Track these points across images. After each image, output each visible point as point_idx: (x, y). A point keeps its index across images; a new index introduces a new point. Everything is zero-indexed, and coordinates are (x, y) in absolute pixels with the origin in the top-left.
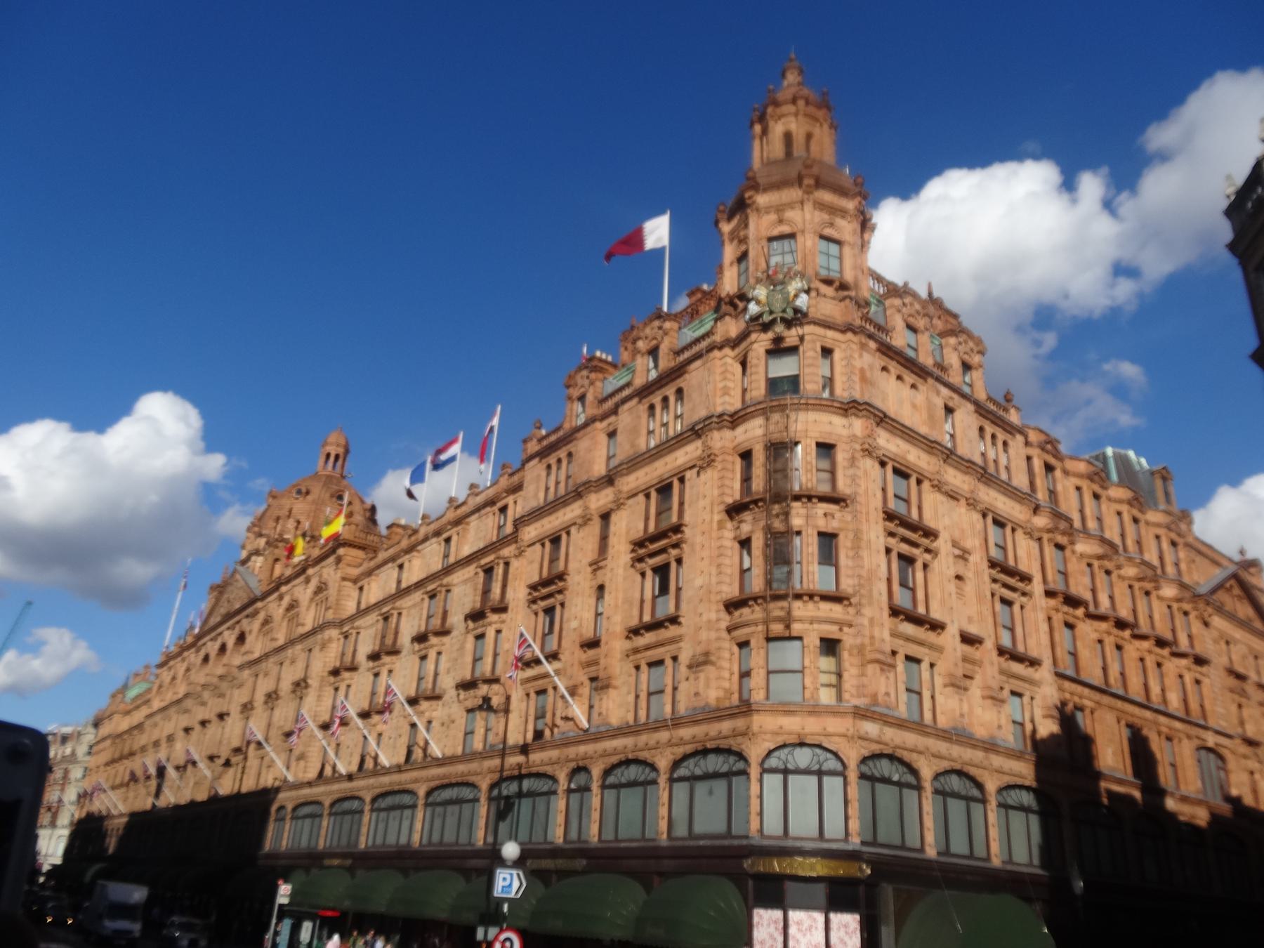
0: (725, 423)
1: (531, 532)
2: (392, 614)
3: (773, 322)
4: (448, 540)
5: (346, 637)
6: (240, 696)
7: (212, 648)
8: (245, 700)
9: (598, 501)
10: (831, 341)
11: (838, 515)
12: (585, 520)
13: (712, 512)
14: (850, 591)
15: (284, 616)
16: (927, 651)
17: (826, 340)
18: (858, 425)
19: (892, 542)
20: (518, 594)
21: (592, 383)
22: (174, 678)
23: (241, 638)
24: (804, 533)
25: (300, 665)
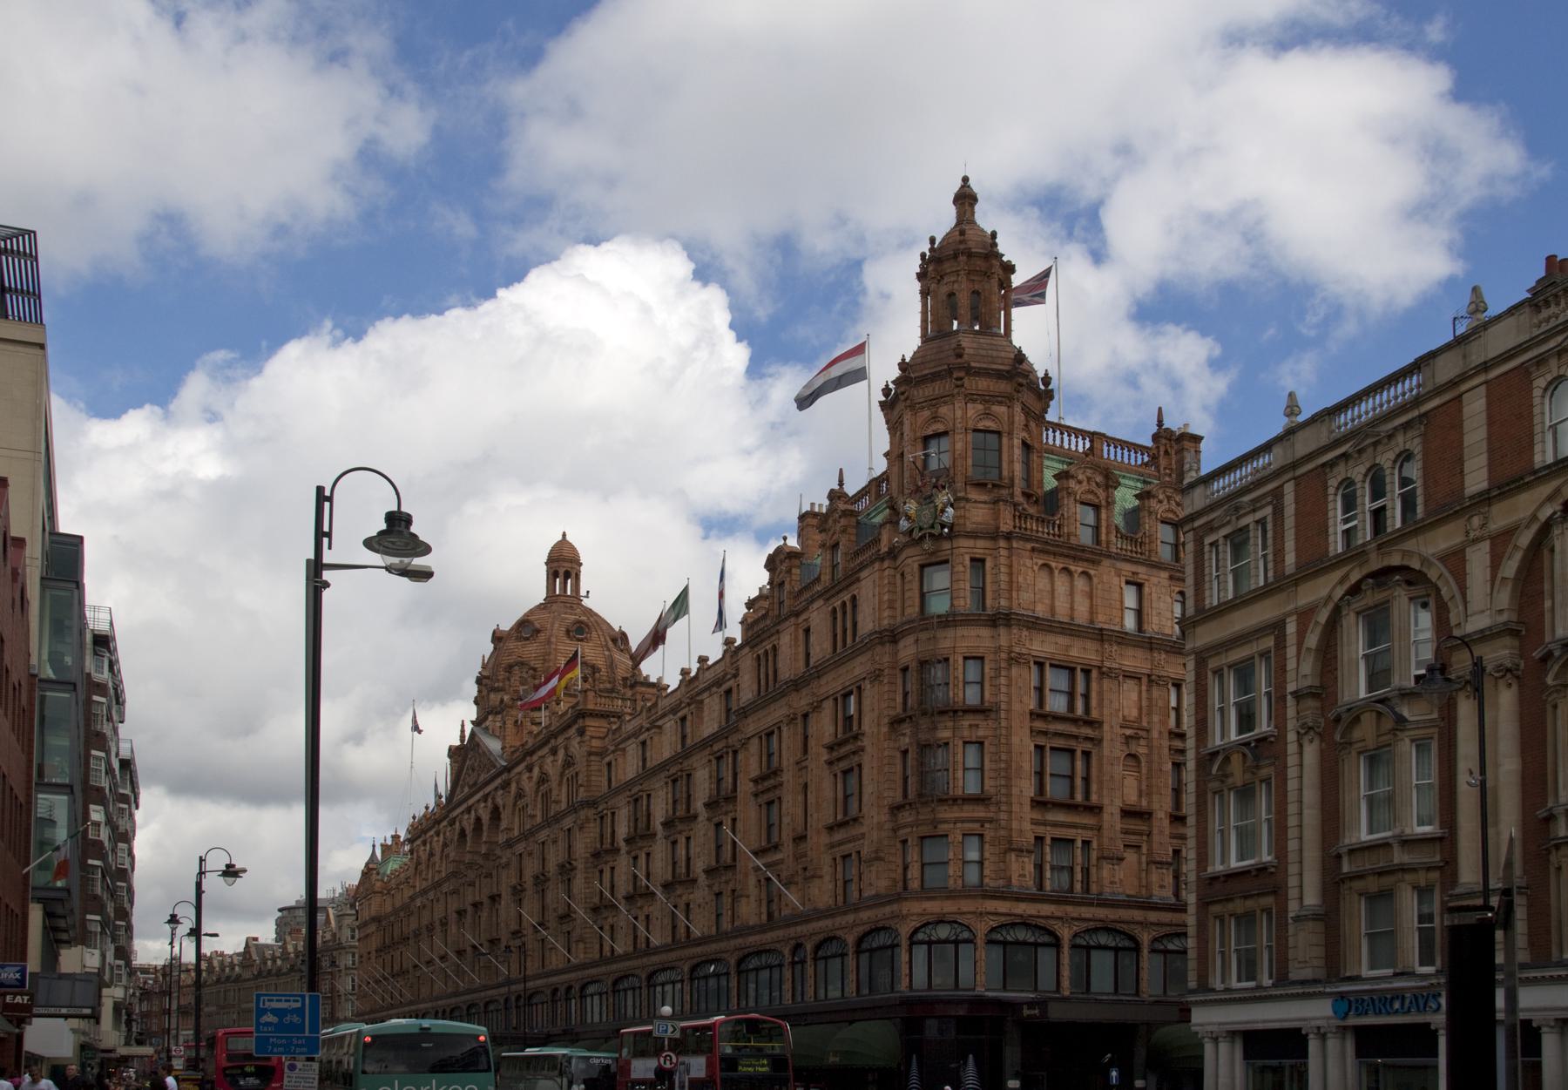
0: (886, 639)
1: (752, 726)
2: (642, 797)
3: (922, 538)
4: (683, 719)
5: (602, 818)
6: (508, 879)
7: (468, 822)
8: (514, 881)
9: (801, 701)
10: (981, 551)
11: (982, 724)
12: (792, 720)
13: (879, 725)
14: (993, 791)
15: (537, 791)
16: (1080, 831)
17: (975, 550)
18: (1004, 637)
19: (1041, 741)
20: (745, 787)
21: (789, 571)
22: (431, 854)
23: (496, 814)
24: (951, 744)
25: (562, 845)
